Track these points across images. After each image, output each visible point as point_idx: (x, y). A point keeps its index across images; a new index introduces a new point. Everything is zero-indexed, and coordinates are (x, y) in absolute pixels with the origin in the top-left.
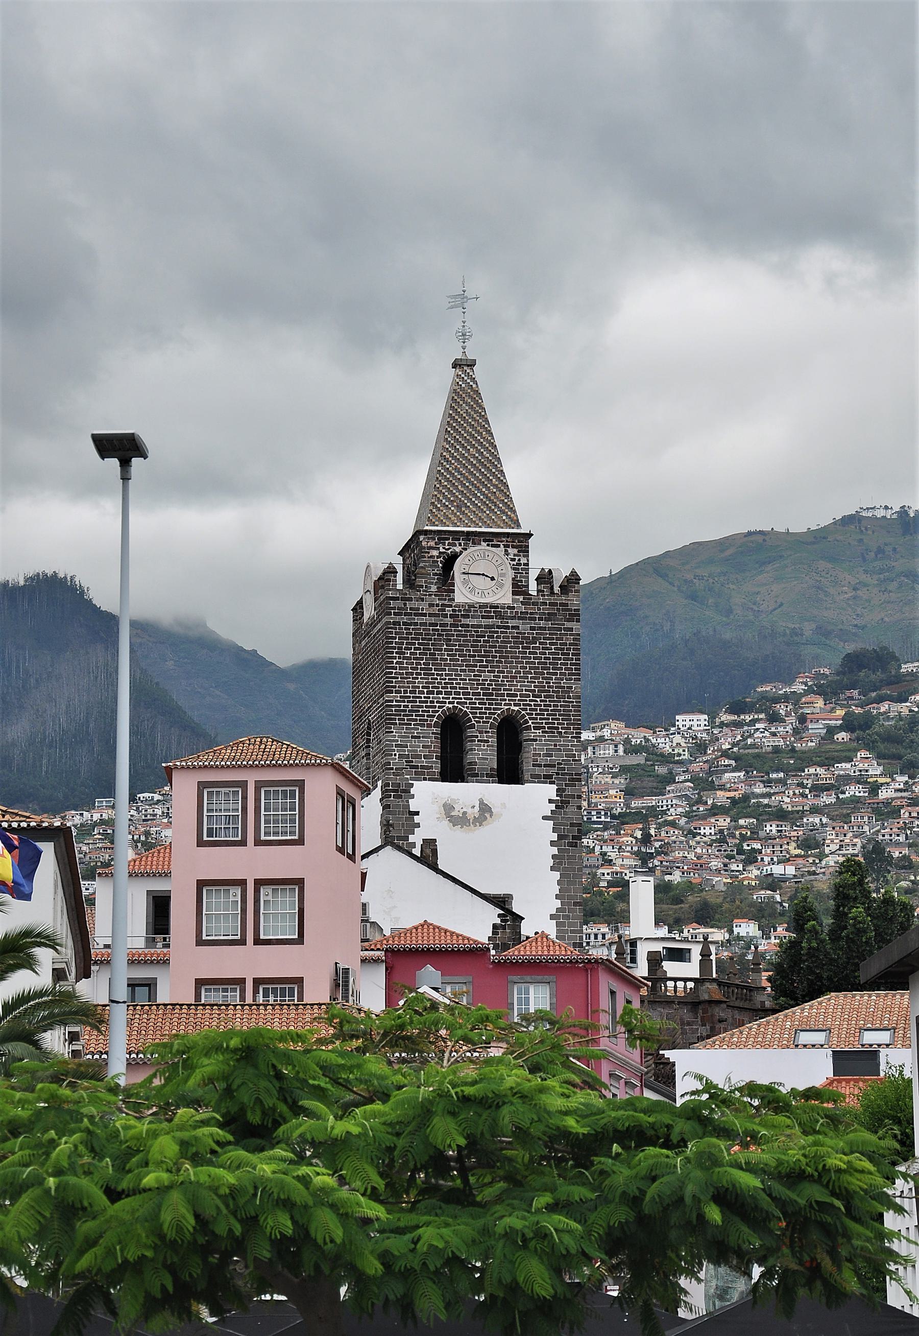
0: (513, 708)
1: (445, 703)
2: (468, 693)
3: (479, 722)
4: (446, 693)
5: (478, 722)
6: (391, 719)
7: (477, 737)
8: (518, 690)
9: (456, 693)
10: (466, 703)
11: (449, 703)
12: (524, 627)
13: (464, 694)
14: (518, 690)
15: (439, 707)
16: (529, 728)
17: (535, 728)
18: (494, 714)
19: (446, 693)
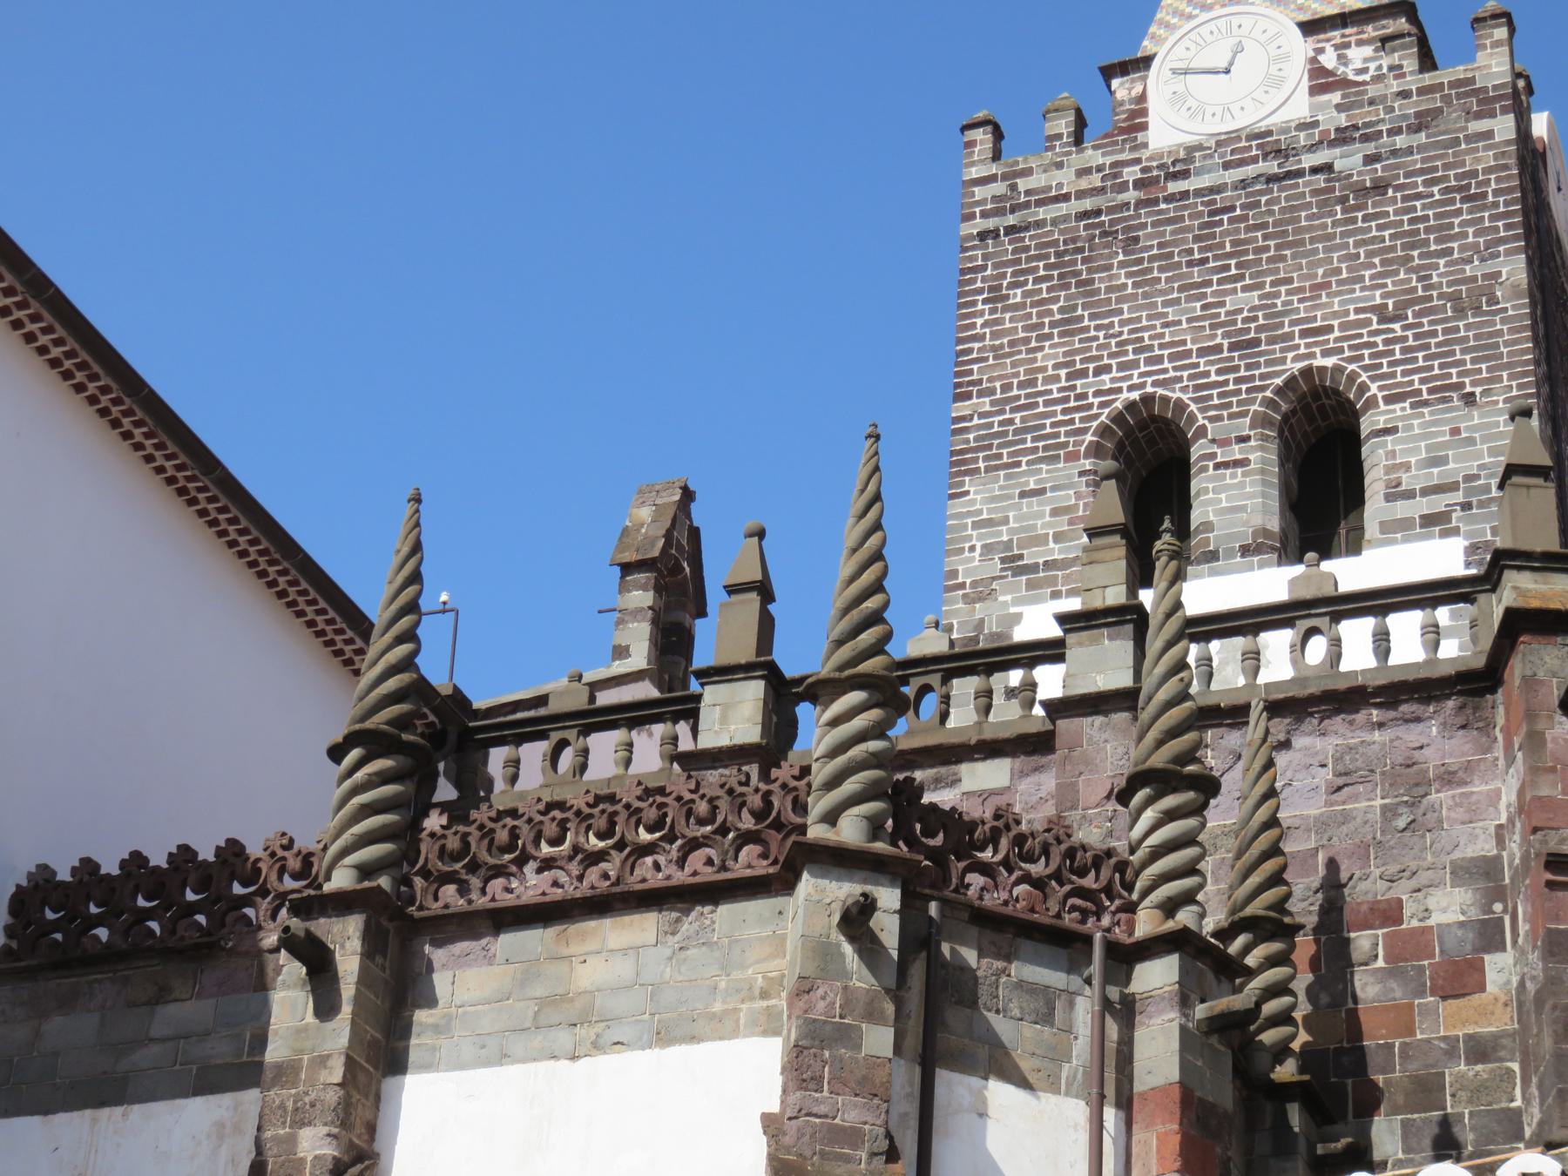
0: (1319, 362)
1: (1120, 390)
2: (1188, 354)
3: (1219, 418)
4: (1121, 366)
5: (1212, 419)
6: (964, 462)
7: (1213, 455)
8: (1335, 315)
9: (1149, 361)
10: (1180, 379)
11: (1131, 388)
12: (1349, 161)
13: (1172, 358)
14: (1335, 315)
15: (1102, 405)
16: (1372, 403)
17: (1389, 400)
18: (1263, 388)
19: (1121, 366)
